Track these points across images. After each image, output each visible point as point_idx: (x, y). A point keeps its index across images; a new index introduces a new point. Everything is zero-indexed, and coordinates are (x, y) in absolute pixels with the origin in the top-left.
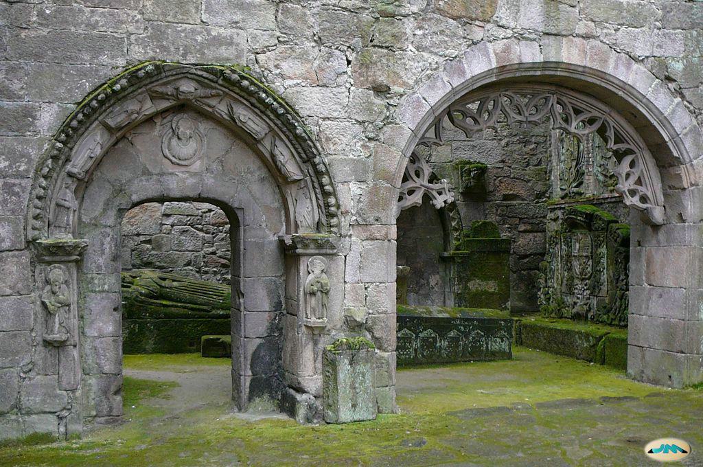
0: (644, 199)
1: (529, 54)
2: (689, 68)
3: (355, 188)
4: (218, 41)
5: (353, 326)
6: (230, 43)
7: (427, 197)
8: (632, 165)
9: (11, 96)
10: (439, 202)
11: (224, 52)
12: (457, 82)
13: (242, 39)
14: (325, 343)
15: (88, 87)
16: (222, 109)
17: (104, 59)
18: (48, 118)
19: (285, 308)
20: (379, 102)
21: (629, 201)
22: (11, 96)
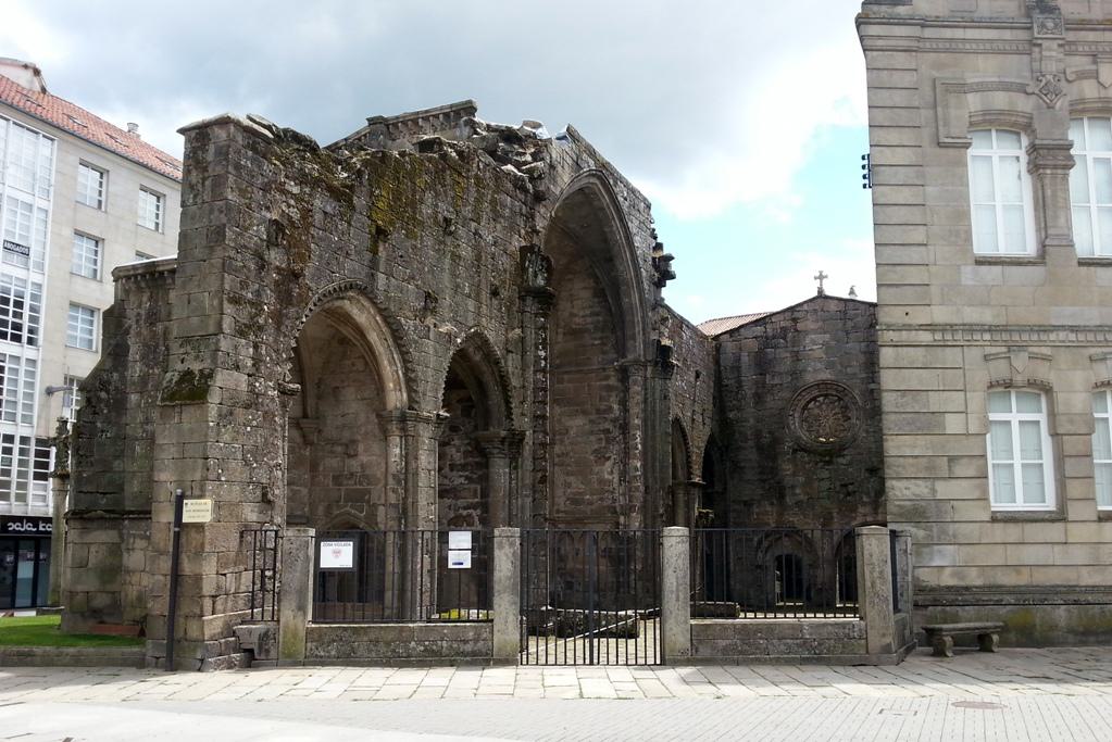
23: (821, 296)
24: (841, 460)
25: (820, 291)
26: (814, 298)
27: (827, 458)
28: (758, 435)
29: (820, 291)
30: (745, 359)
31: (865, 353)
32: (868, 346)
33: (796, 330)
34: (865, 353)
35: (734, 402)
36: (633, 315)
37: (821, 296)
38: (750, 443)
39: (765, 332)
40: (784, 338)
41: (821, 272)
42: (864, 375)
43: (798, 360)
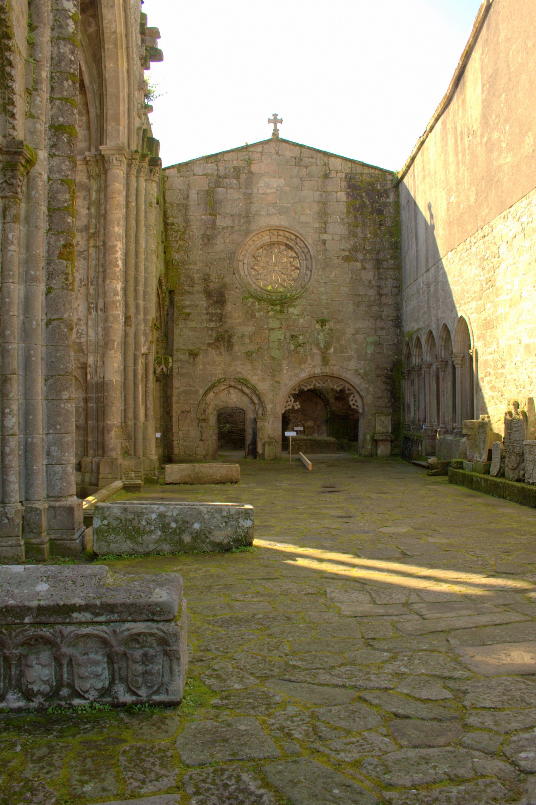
0: (357, 406)
1: (318, 371)
2: (365, 372)
3: (271, 406)
4: (238, 373)
5: (269, 438)
6: (241, 373)
7: (293, 407)
8: (354, 397)
9: (194, 387)
10: (296, 408)
11: (240, 376)
12: (297, 379)
13: (244, 372)
14: (263, 441)
15: (210, 384)
16: (240, 387)
17: (213, 378)
18: (201, 392)
19: (255, 434)
20: (276, 385)
21: (353, 407)
22: (194, 387)
23: (276, 139)
24: (291, 310)
25: (276, 132)
26: (269, 141)
27: (278, 308)
28: (206, 279)
29: (276, 132)
30: (194, 195)
31: (319, 202)
32: (321, 195)
33: (250, 172)
34: (319, 202)
35: (181, 243)
36: (118, 88)
37: (276, 139)
38: (197, 288)
39: (218, 170)
40: (238, 178)
41: (275, 115)
42: (317, 225)
43: (251, 203)
